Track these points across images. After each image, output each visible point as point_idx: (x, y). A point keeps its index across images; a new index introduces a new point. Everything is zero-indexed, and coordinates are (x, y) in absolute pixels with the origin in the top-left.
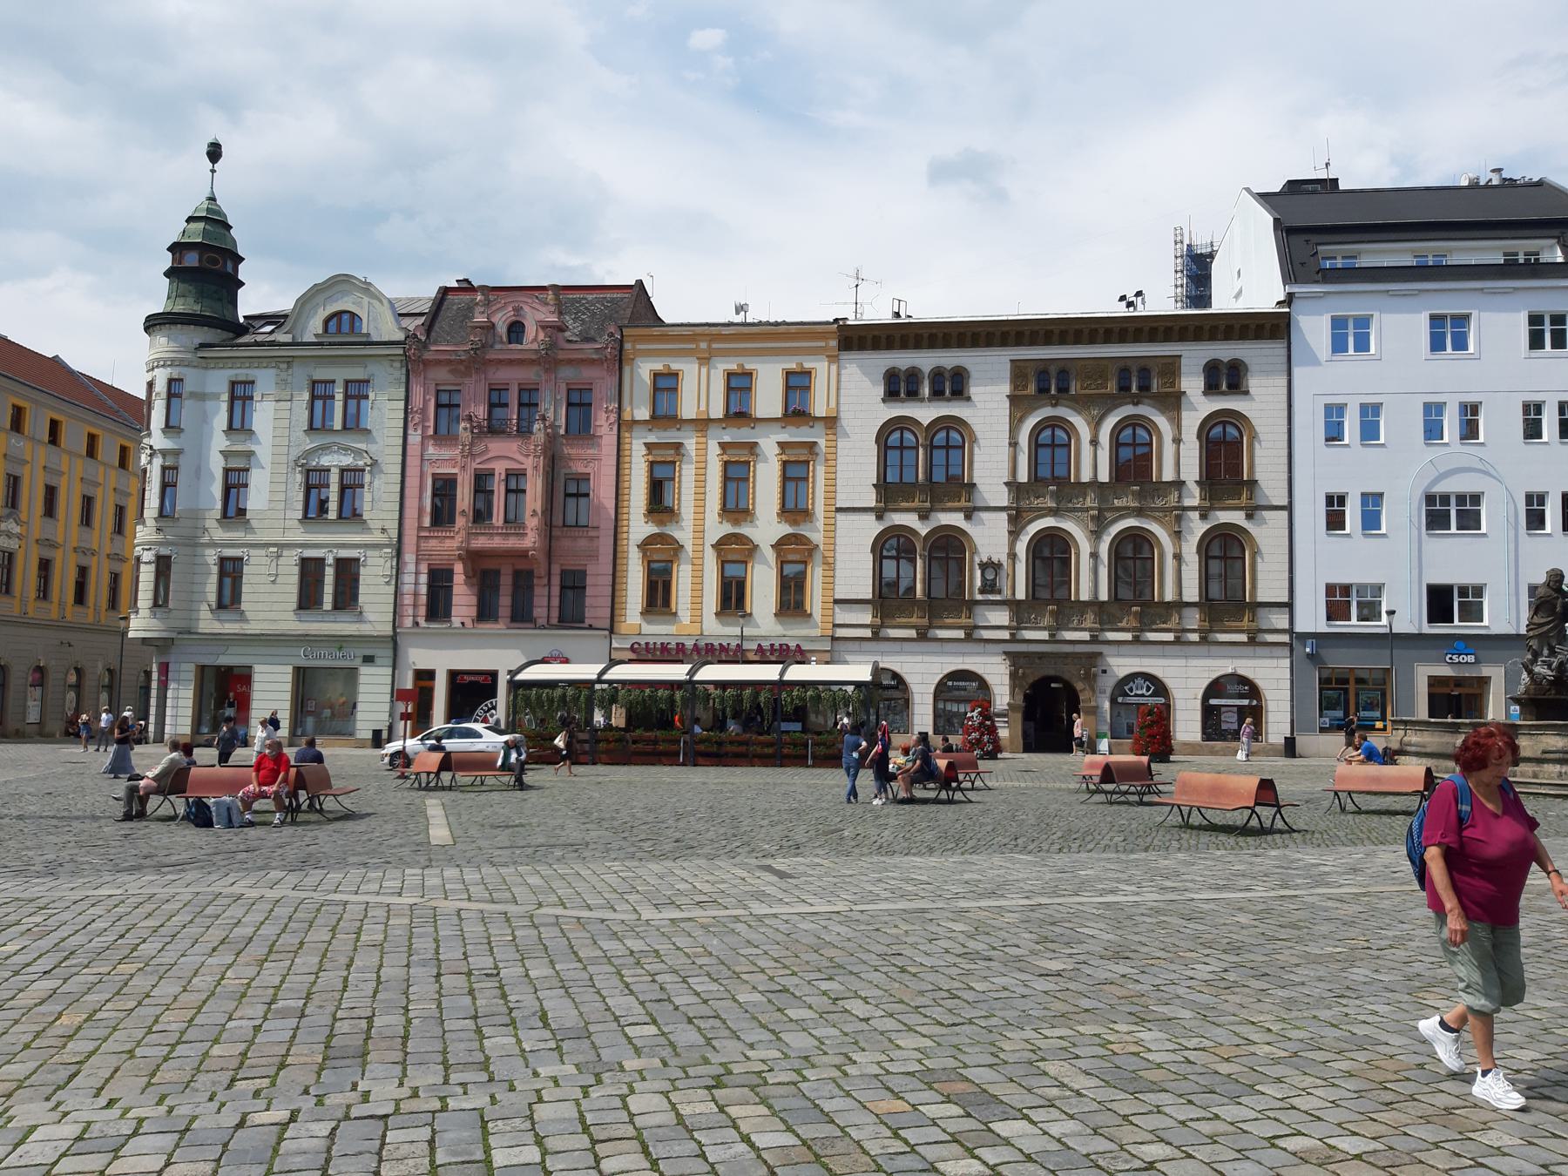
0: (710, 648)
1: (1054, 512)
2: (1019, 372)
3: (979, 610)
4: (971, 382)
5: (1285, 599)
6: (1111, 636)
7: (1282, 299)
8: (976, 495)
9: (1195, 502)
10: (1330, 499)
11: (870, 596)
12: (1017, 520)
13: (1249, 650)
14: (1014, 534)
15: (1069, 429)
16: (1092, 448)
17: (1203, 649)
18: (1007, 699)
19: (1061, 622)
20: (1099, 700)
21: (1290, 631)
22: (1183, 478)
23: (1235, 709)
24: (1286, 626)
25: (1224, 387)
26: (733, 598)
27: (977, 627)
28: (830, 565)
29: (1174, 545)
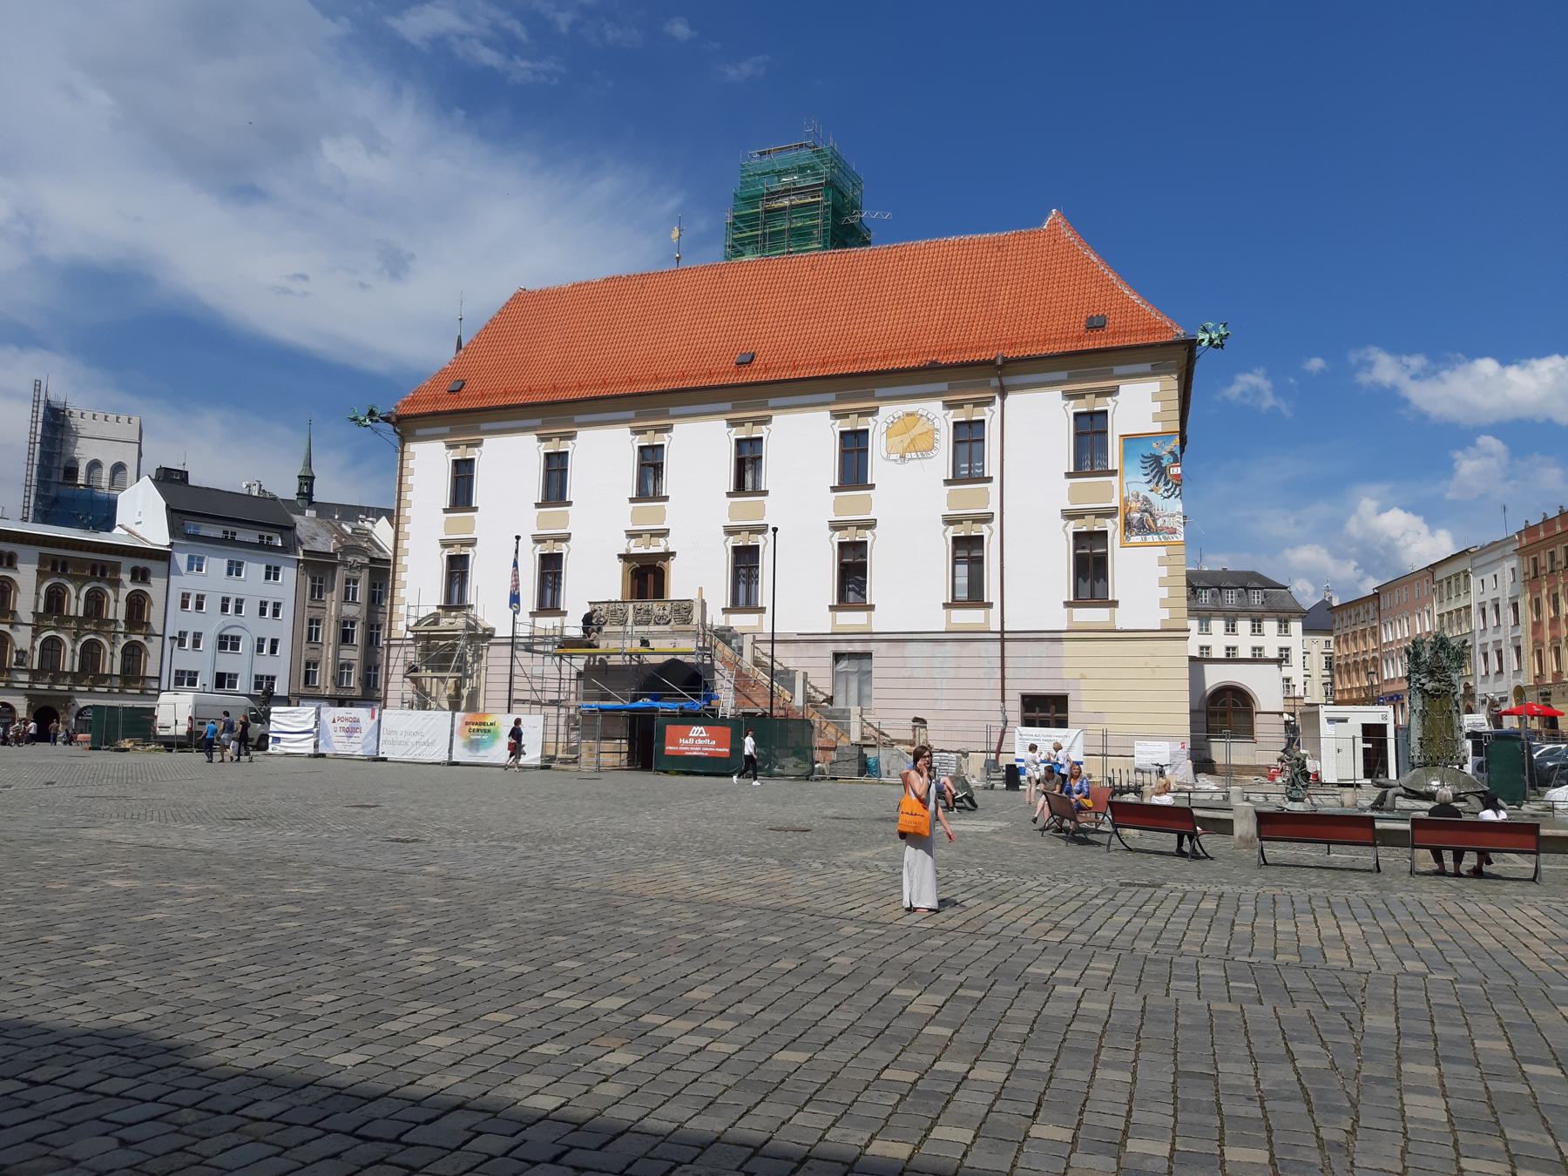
1: (54, 628)
2: (43, 560)
3: (13, 673)
4: (18, 560)
6: (78, 688)
9: (122, 630)
14: (34, 638)
15: (66, 590)
19: (55, 681)
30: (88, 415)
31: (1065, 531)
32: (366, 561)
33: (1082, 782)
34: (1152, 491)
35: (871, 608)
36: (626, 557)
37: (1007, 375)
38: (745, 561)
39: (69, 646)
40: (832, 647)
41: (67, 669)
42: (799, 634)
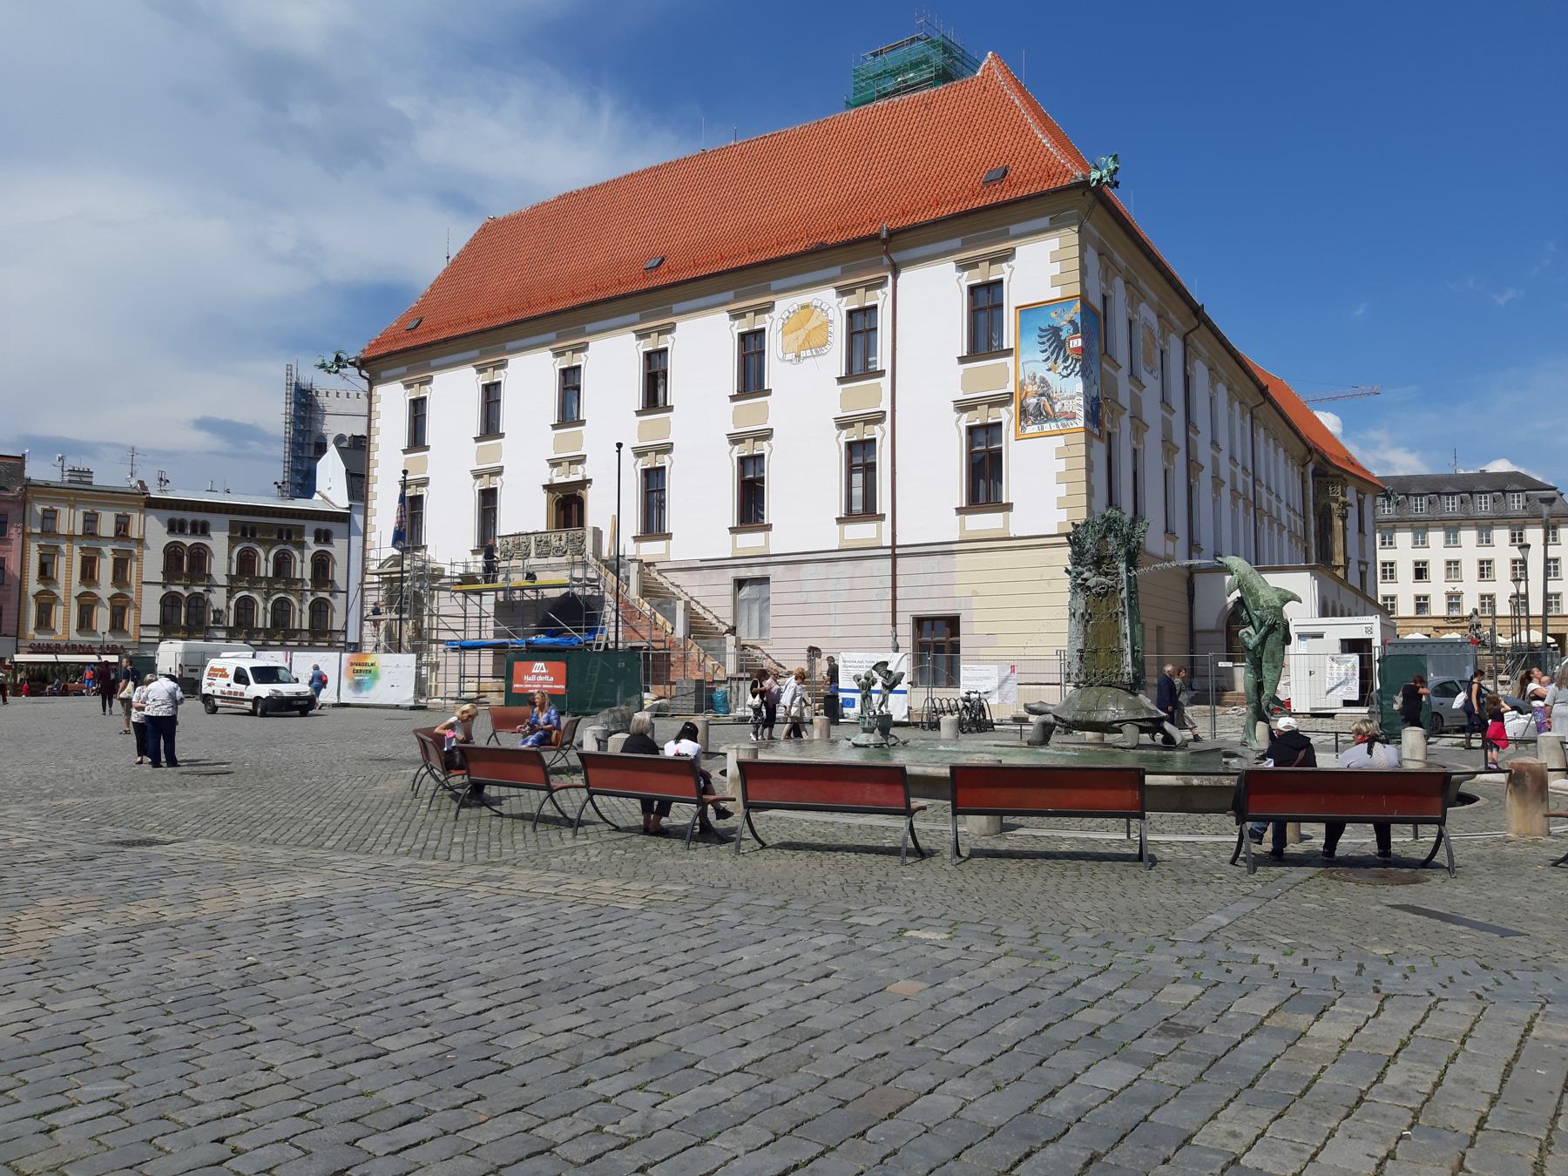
0: (74, 647)
2: (233, 527)
11: (158, 623)
14: (229, 598)
15: (256, 553)
26: (85, 623)
28: (138, 608)
30: (332, 394)
31: (957, 426)
33: (550, 713)
34: (1049, 370)
35: (768, 527)
36: (549, 488)
37: (895, 251)
38: (654, 482)
39: (261, 605)
40: (733, 574)
41: (260, 626)
42: (701, 561)
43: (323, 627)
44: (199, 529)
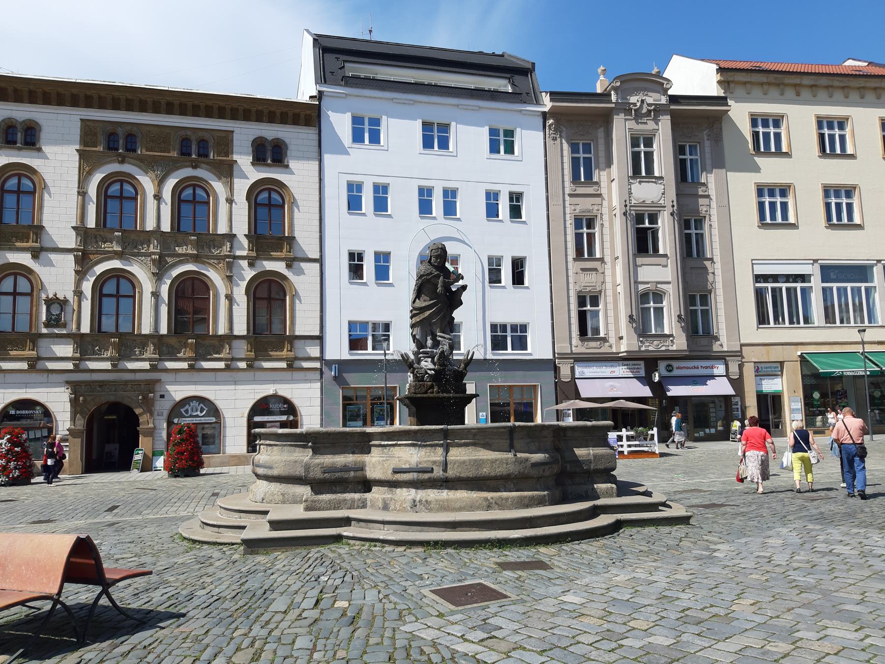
1: (119, 255)
3: (42, 343)
4: (44, 135)
5: (317, 333)
7: (314, 94)
8: (44, 237)
9: (244, 253)
10: (352, 255)
12: (84, 262)
13: (288, 375)
14: (81, 274)
16: (156, 202)
17: (250, 374)
18: (68, 425)
20: (157, 422)
21: (321, 359)
22: (234, 232)
23: (279, 424)
24: (318, 355)
25: (269, 161)
27: (39, 358)
29: (226, 287)
32: (664, 100)
43: (276, 329)
44: (19, 136)
